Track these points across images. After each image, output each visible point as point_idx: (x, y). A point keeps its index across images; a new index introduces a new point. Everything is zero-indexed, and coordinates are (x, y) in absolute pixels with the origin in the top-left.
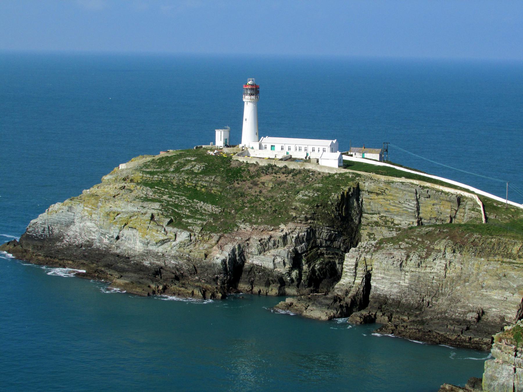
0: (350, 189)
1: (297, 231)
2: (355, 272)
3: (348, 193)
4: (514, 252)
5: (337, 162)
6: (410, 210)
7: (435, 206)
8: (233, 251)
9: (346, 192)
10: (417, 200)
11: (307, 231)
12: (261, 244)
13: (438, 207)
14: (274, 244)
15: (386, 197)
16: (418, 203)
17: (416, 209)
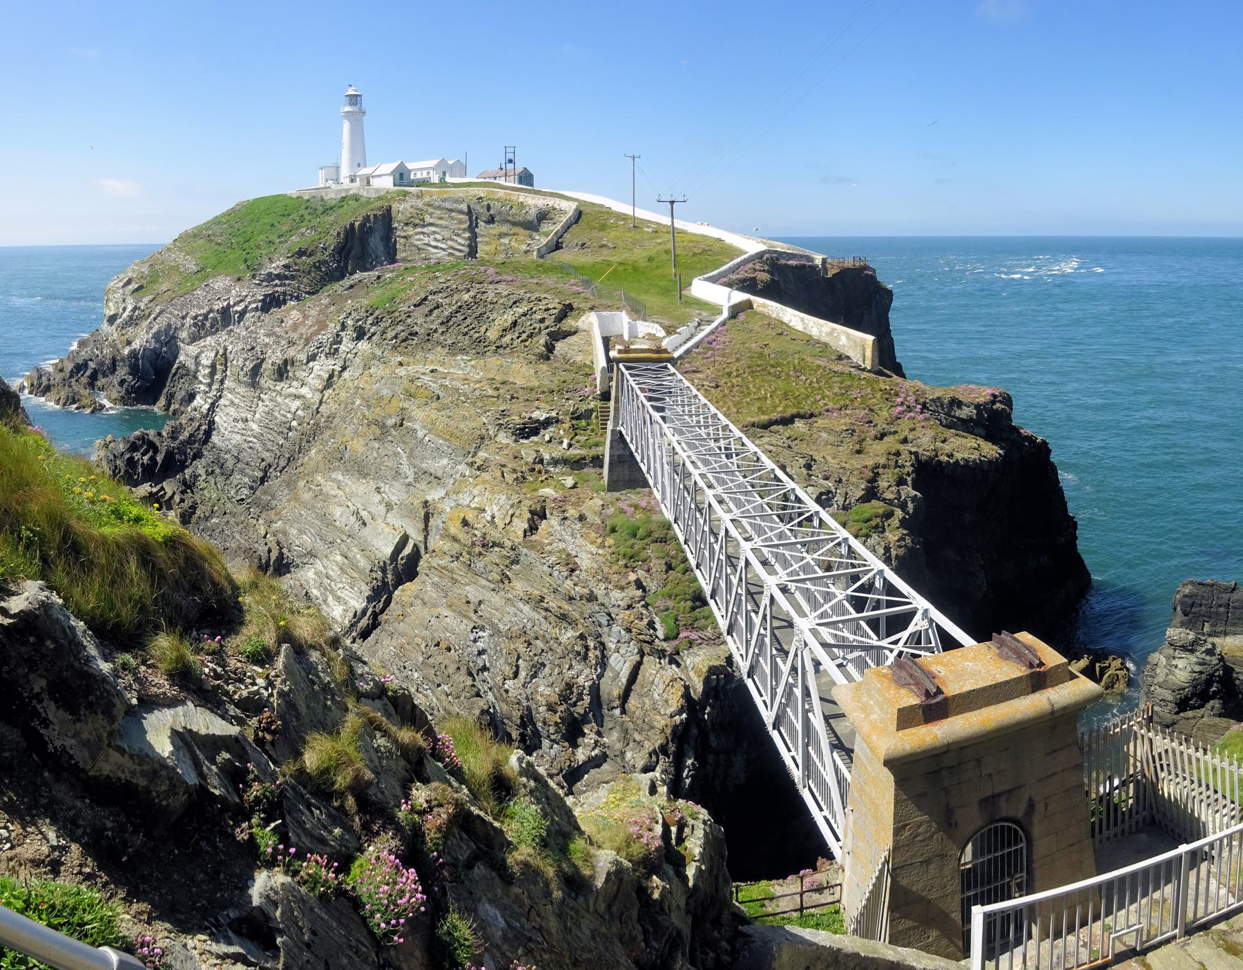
0: (367, 218)
1: (249, 299)
2: (210, 385)
3: (362, 225)
4: (492, 335)
5: (391, 178)
6: (458, 254)
7: (502, 240)
8: (156, 336)
9: (357, 224)
10: (472, 228)
11: (262, 301)
12: (195, 325)
13: (505, 241)
14: (212, 327)
15: (425, 230)
16: (474, 236)
17: (466, 250)
